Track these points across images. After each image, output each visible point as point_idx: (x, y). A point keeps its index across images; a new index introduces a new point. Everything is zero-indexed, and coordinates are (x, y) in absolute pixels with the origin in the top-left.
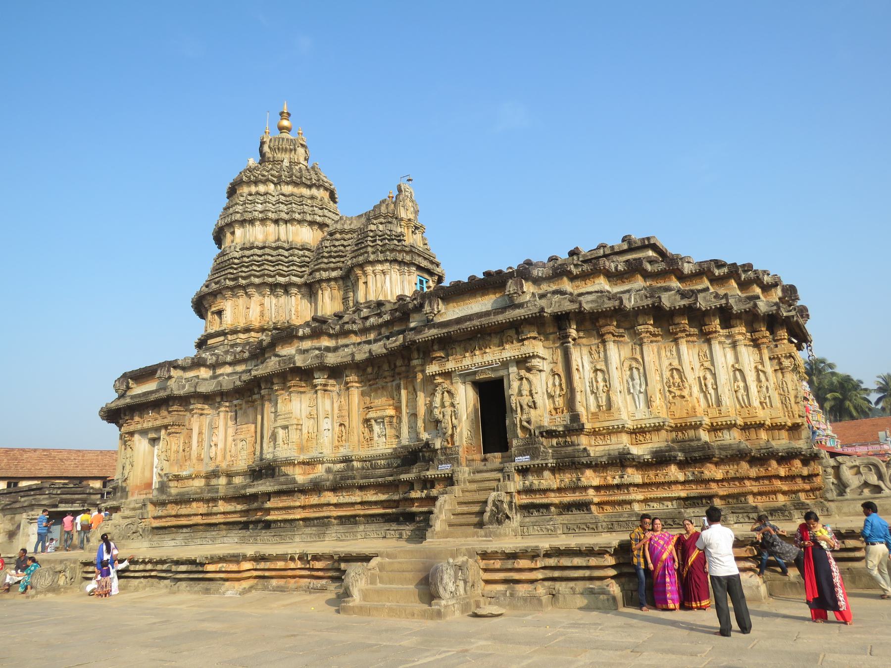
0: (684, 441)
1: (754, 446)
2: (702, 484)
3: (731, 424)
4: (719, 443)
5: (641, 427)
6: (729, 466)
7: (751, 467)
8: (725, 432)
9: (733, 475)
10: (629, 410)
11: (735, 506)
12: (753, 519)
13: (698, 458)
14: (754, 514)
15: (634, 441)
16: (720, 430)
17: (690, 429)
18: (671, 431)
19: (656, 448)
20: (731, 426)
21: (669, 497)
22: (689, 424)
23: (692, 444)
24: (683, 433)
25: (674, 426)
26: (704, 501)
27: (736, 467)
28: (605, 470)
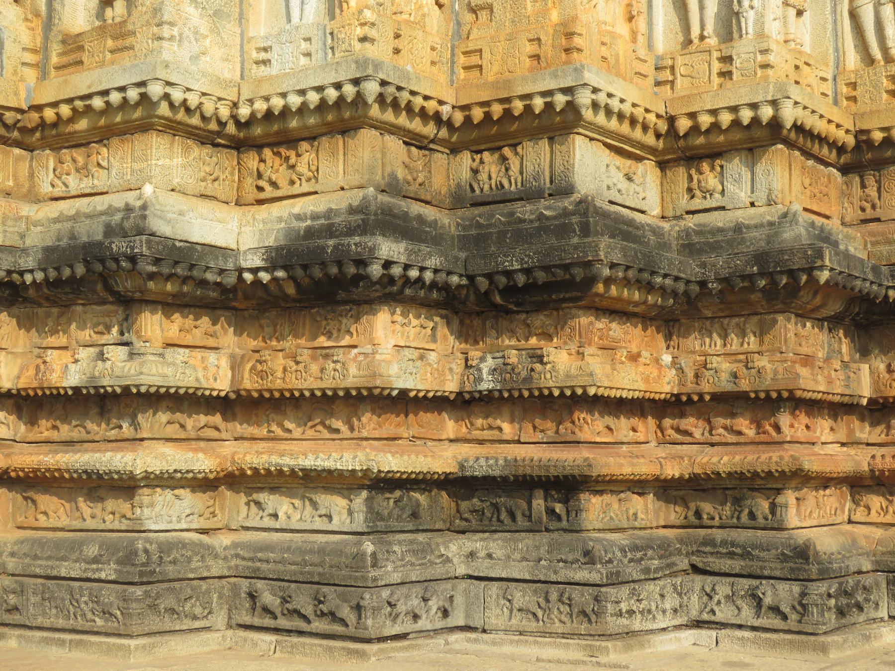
0: (502, 198)
1: (884, 249)
2: (544, 417)
3: (755, 121)
4: (691, 222)
5: (269, 115)
6: (724, 336)
7: (865, 353)
8: (735, 166)
9: (725, 384)
10: (252, 33)
11: (718, 535)
12: (775, 610)
13: (521, 279)
14: (782, 586)
15: (249, 182)
16: (714, 154)
17: (534, 135)
18: (454, 150)
19: (315, 217)
20: (757, 133)
21: (330, 472)
22: (518, 106)
23: (525, 211)
24: (504, 159)
25: (459, 118)
26: (539, 503)
27: (752, 341)
28: (63, 320)
